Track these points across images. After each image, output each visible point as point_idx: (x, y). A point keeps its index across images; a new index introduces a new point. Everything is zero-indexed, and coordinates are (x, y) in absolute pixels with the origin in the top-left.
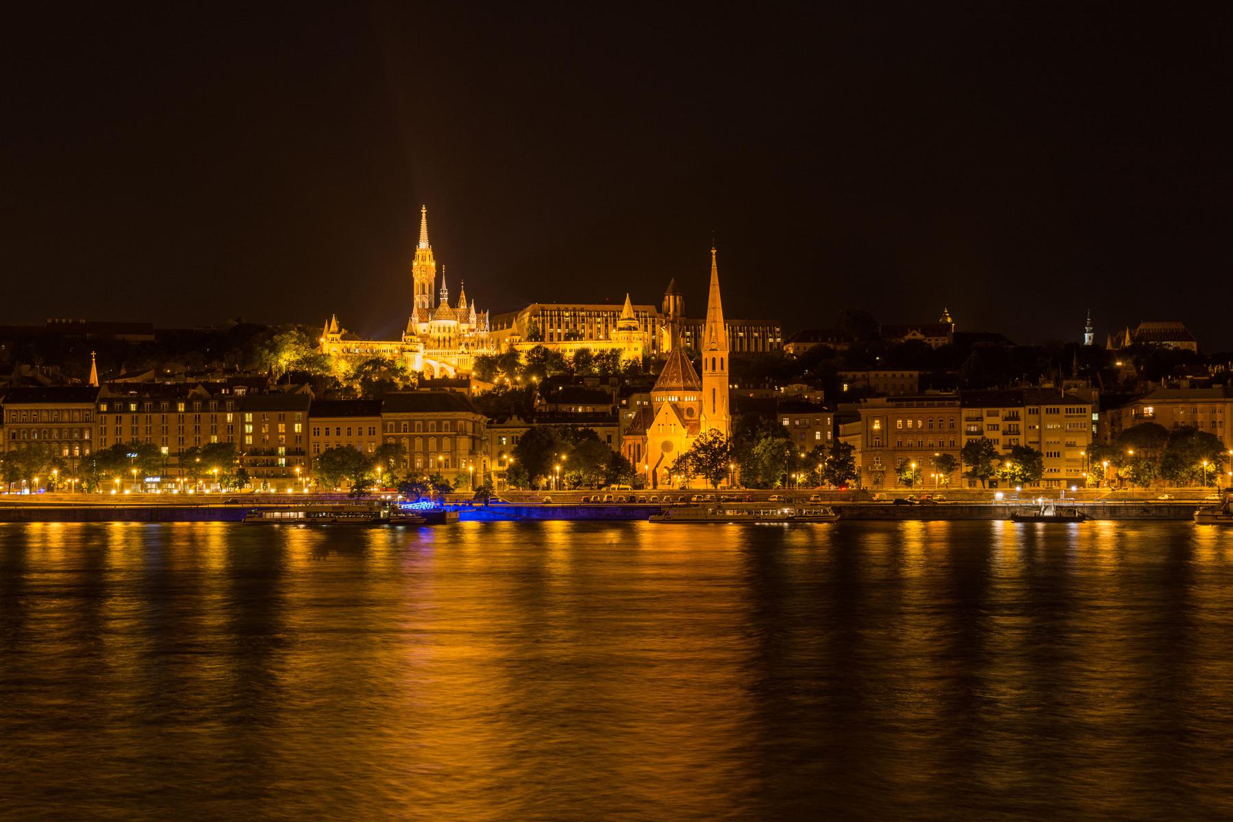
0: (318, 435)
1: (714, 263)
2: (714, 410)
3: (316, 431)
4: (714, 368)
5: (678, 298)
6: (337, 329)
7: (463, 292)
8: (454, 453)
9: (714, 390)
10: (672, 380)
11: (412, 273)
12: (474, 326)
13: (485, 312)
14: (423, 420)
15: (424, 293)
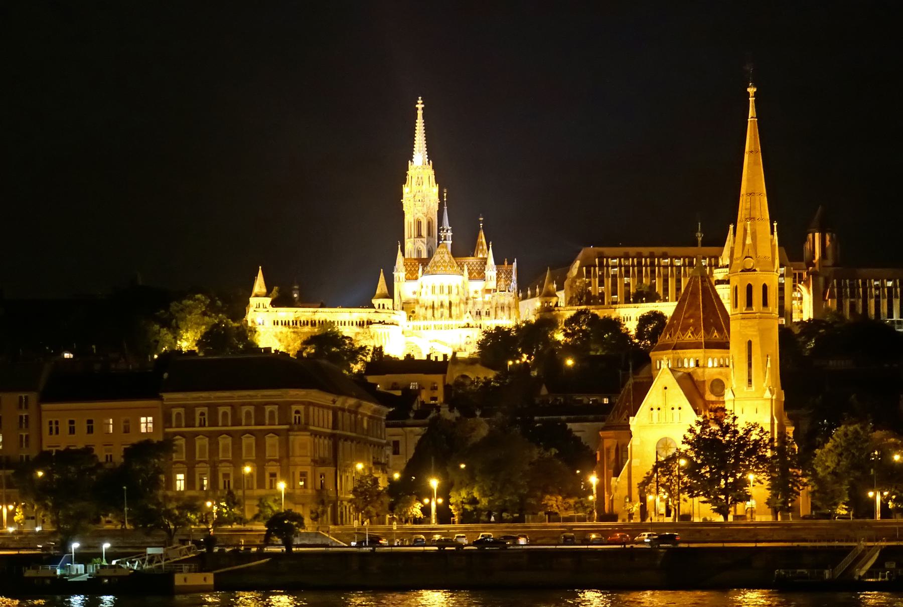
0: (57, 432)
1: (752, 112)
2: (750, 381)
3: (54, 426)
4: (749, 304)
5: (828, 237)
6: (264, 290)
7: (482, 234)
8: (285, 461)
9: (750, 343)
10: (684, 330)
11: (402, 204)
12: (492, 285)
13: (510, 263)
14: (232, 406)
15: (419, 235)
